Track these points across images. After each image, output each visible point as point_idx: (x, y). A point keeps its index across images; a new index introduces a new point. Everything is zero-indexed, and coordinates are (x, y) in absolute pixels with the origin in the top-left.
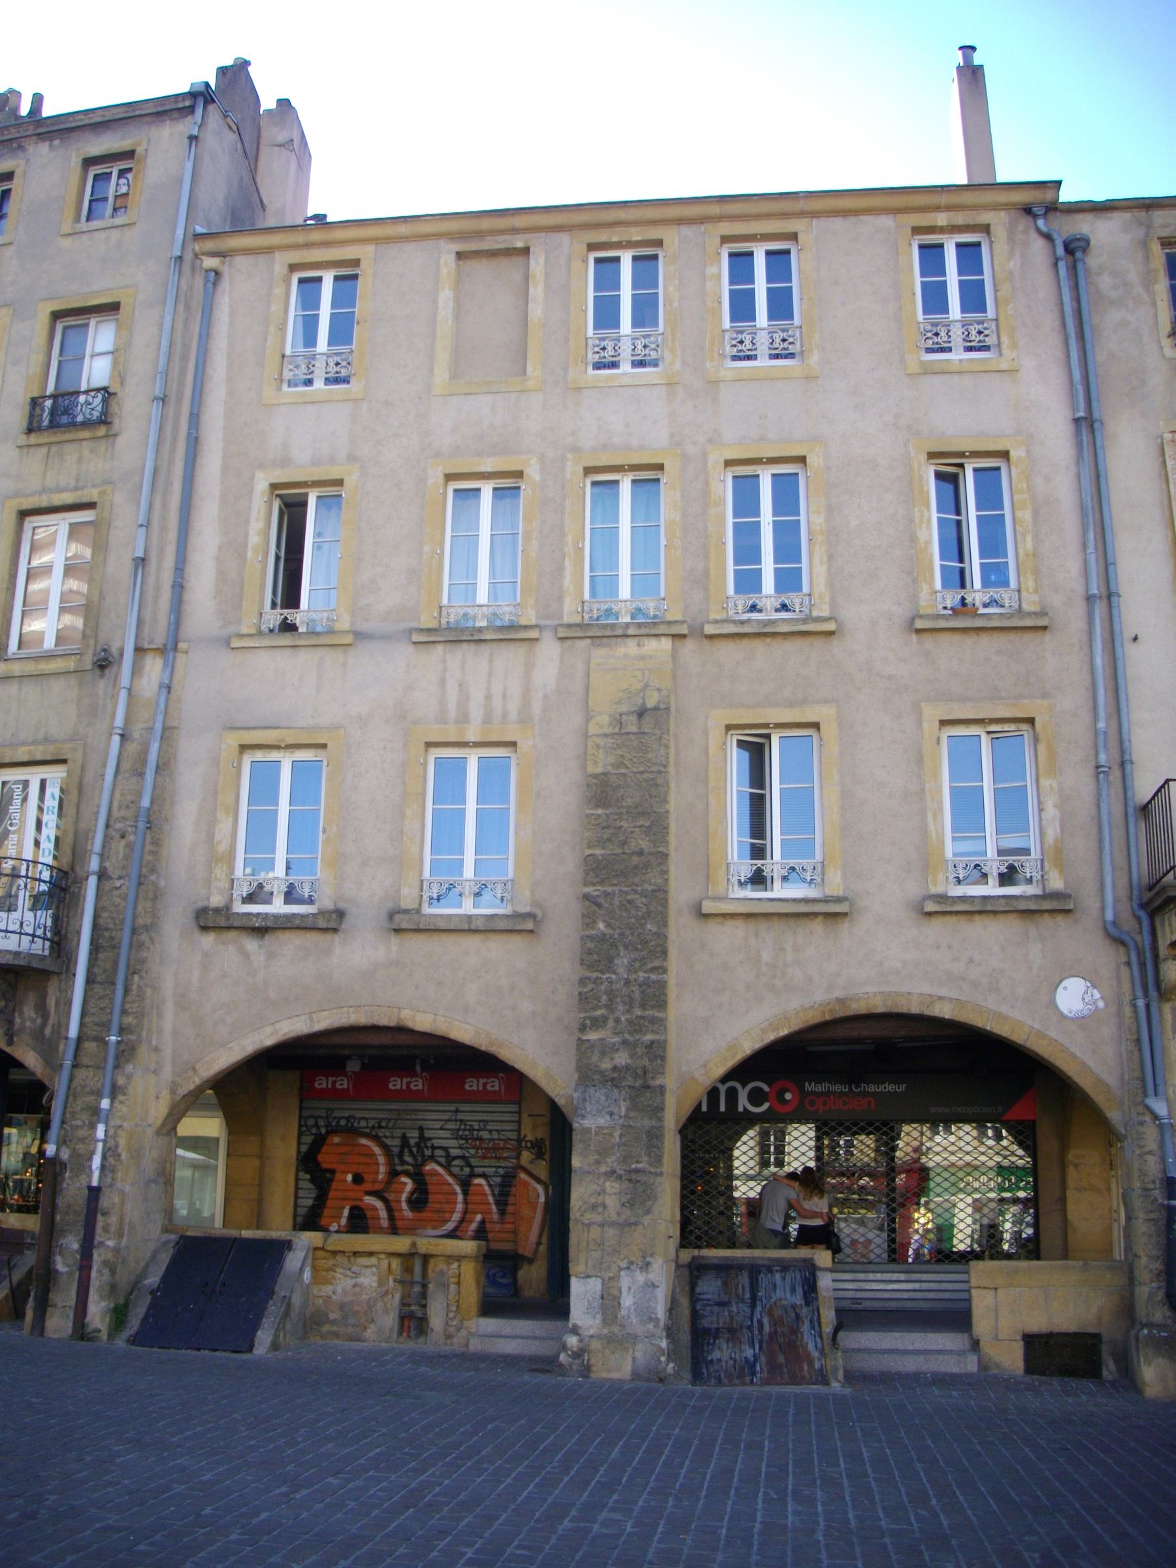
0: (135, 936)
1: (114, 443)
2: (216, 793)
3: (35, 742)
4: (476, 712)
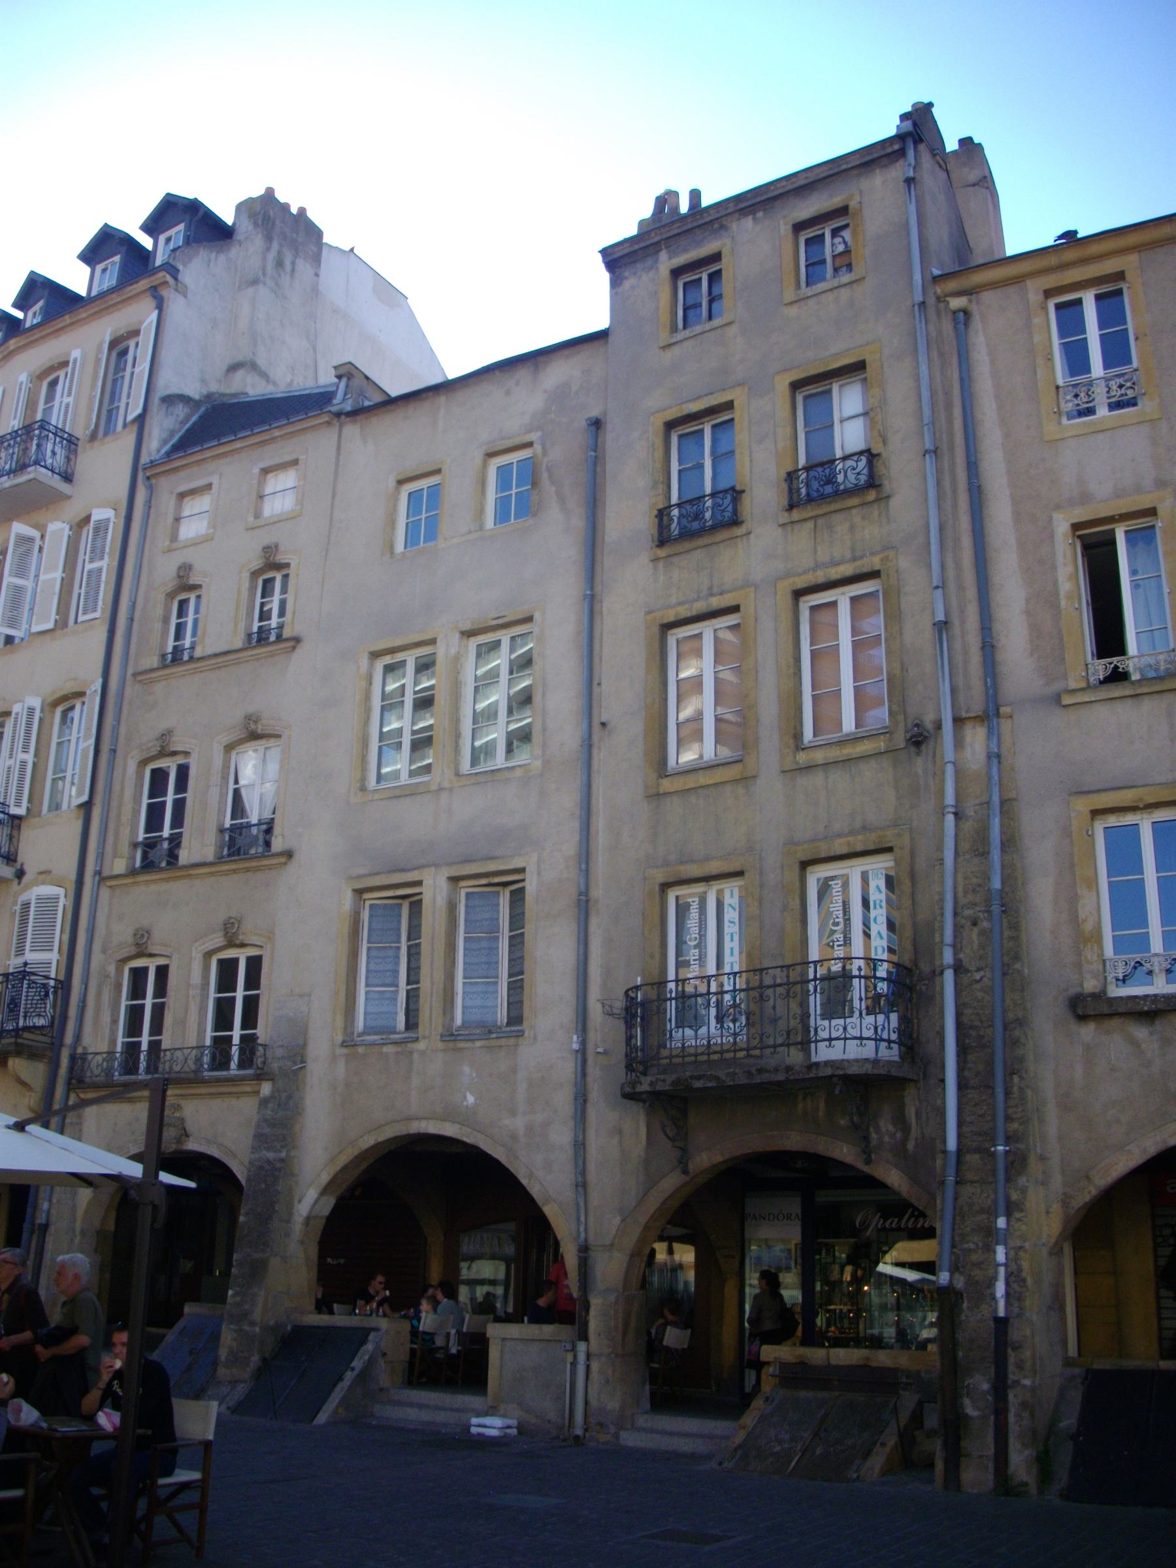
0: (1007, 1032)
1: (887, 504)
2: (1072, 866)
3: (852, 833)
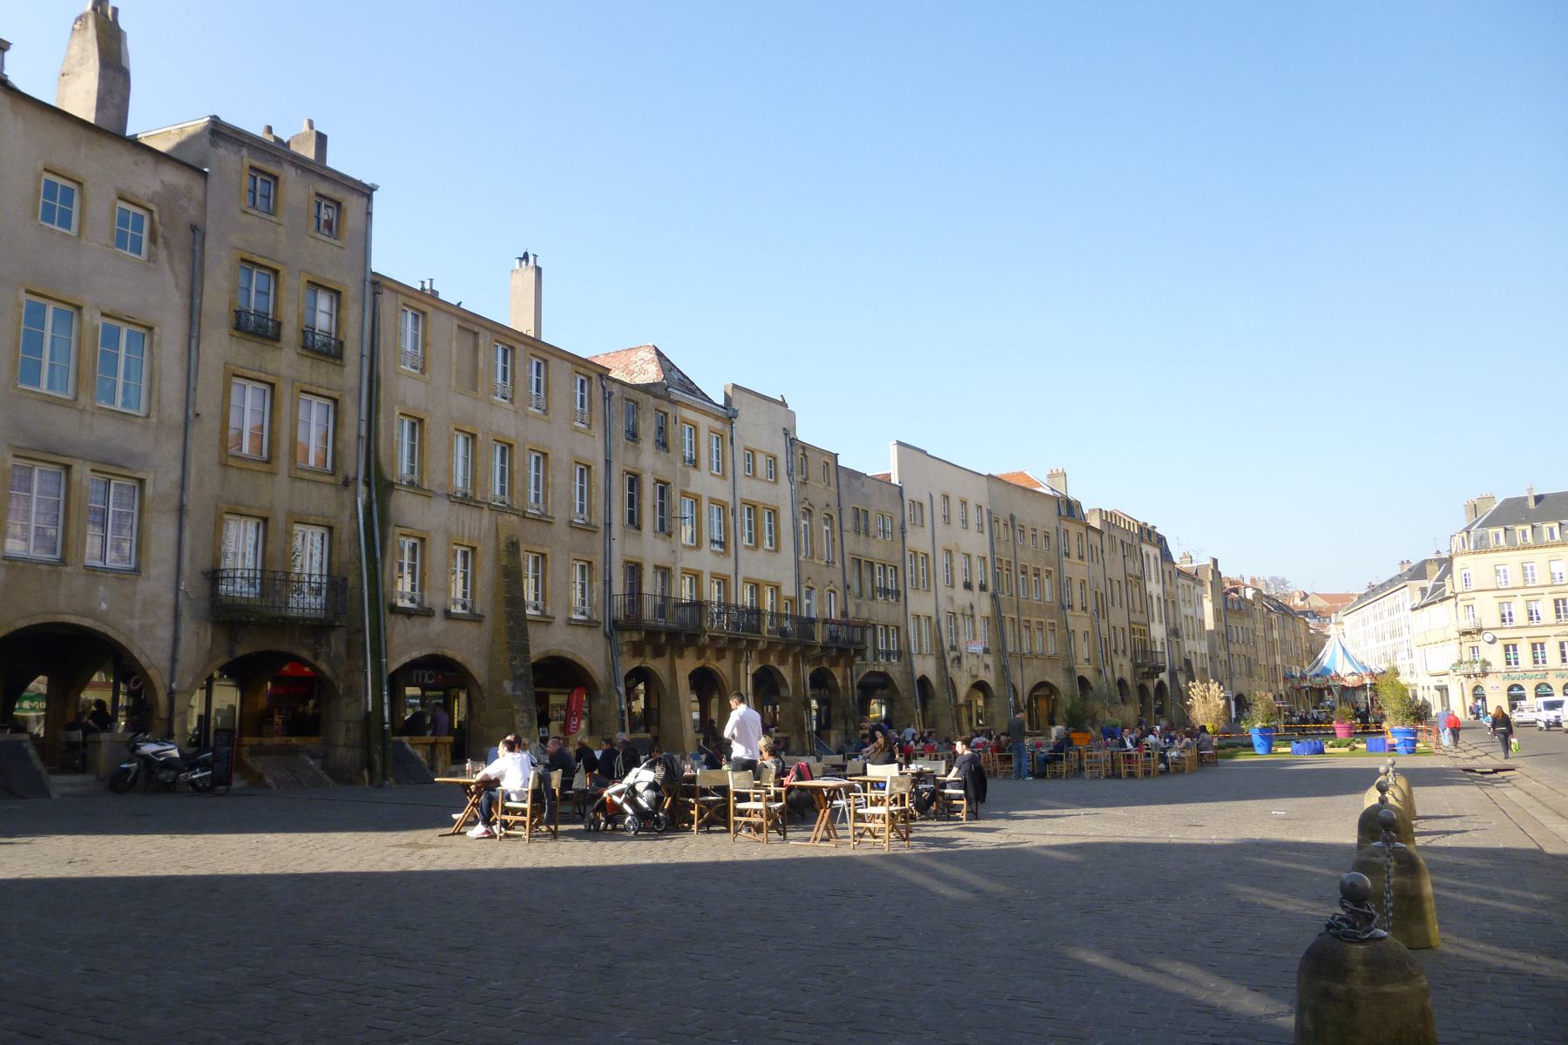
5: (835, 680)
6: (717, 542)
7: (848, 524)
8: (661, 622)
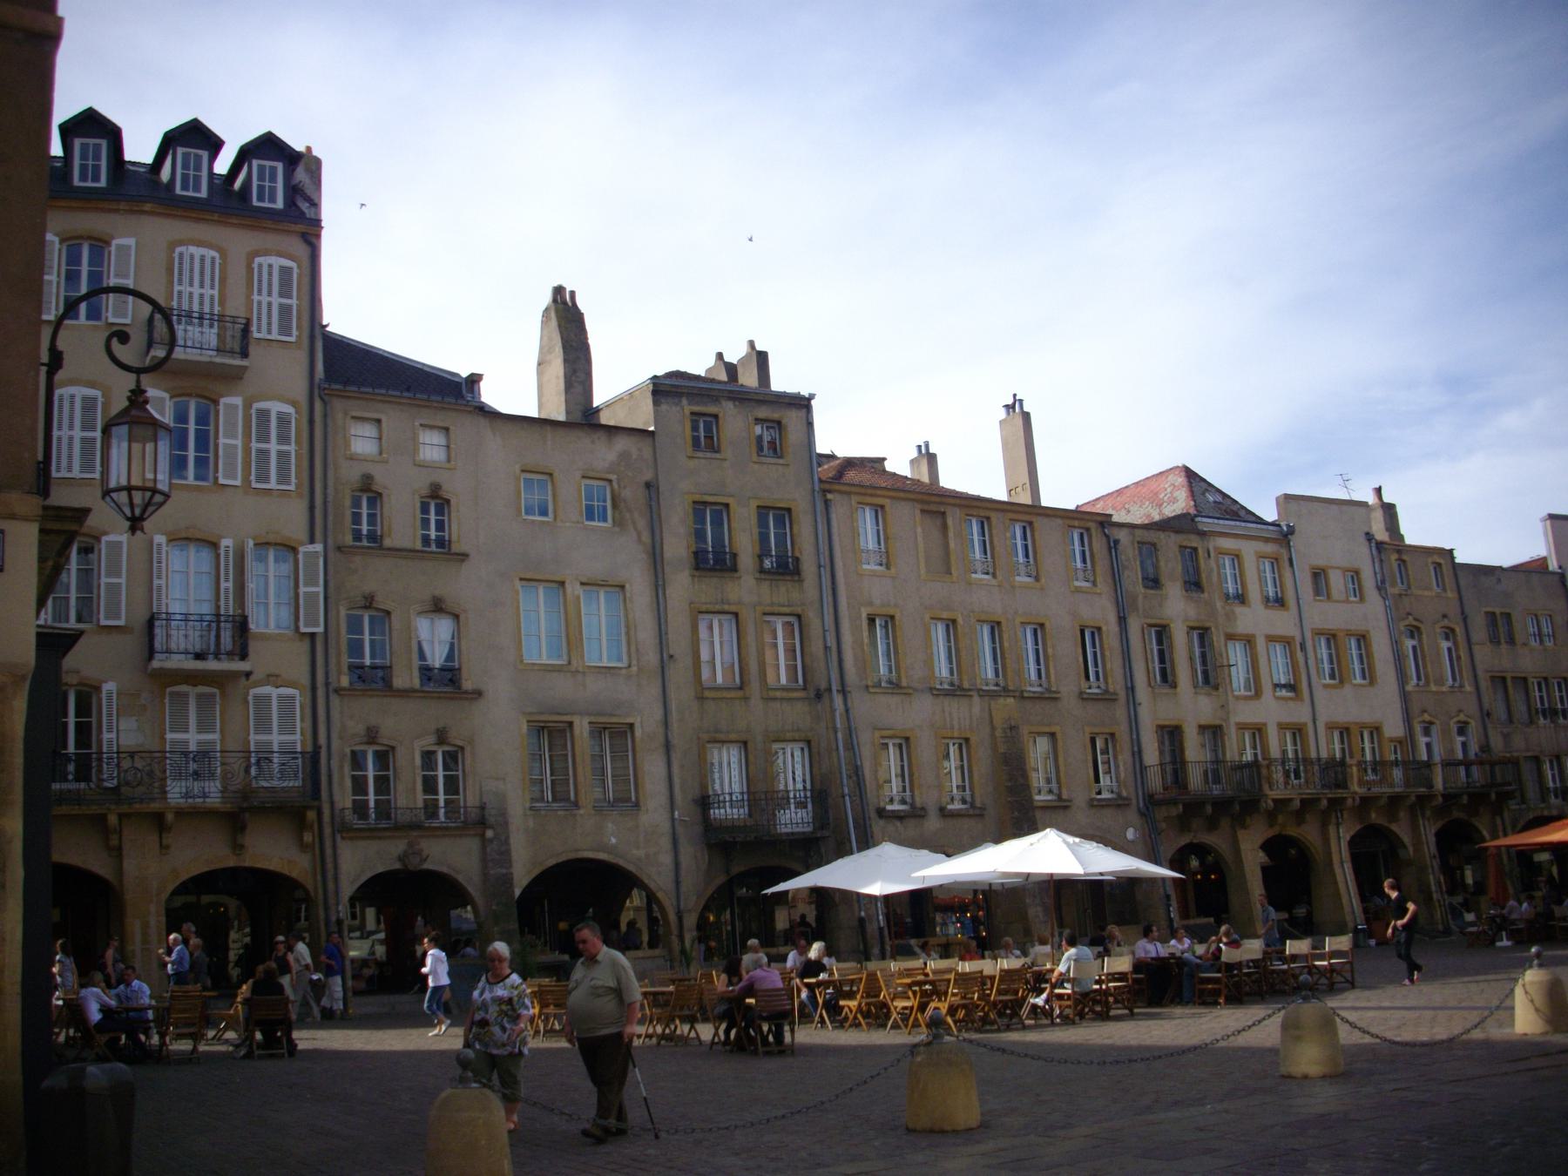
4: (956, 726)
5: (1480, 833)
6: (1284, 686)
7: (1480, 632)
8: (1216, 790)
